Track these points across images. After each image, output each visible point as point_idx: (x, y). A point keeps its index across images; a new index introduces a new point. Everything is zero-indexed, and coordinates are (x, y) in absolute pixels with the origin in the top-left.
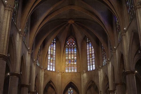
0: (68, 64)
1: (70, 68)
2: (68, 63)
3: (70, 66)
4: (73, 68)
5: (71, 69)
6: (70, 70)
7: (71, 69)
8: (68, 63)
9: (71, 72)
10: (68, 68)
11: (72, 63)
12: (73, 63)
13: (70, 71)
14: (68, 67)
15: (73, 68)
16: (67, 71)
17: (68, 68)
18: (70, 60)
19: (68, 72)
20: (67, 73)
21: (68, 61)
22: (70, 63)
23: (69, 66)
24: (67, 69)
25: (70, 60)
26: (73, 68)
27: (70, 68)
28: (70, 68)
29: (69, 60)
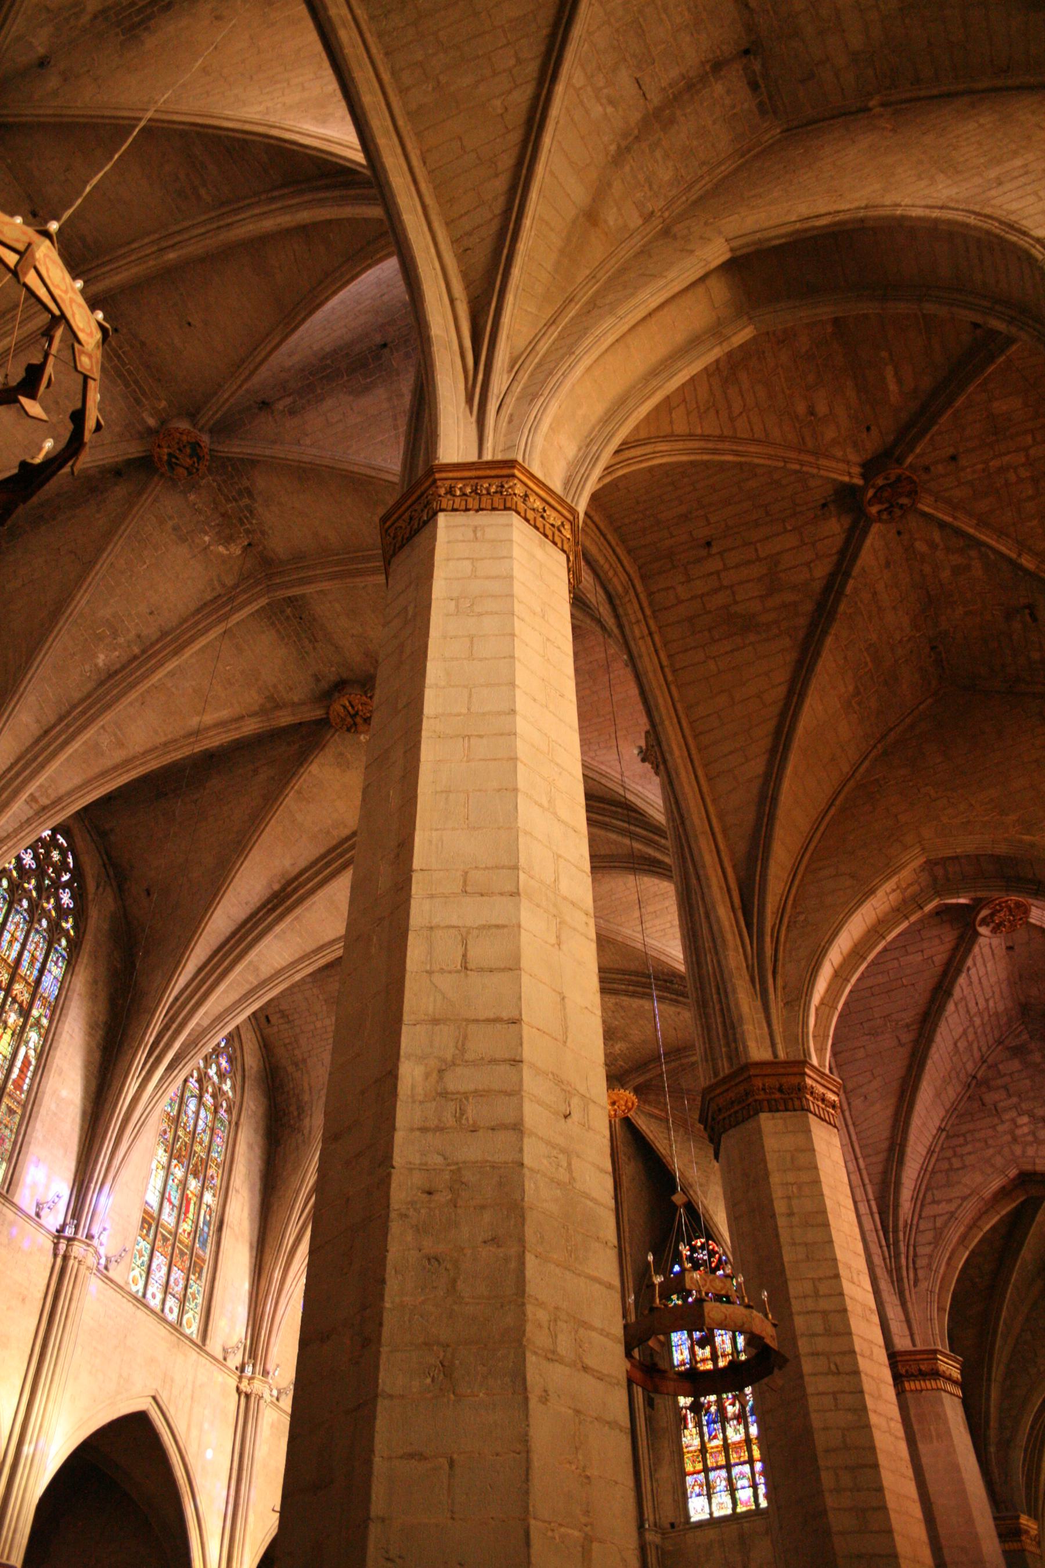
0: (703, 1450)
1: (719, 1478)
2: (701, 1435)
3: (722, 1461)
4: (742, 1476)
5: (732, 1490)
6: (727, 1500)
7: (732, 1490)
8: (697, 1442)
9: (734, 1517)
10: (707, 1477)
11: (730, 1432)
12: (741, 1428)
13: (722, 1506)
14: (706, 1470)
15: (746, 1468)
16: (698, 1509)
17: (707, 1477)
18: (713, 1409)
19: (711, 1514)
20: (701, 1524)
21: (699, 1425)
22: (715, 1437)
23: (710, 1462)
24: (699, 1495)
25: (713, 1409)
26: (746, 1468)
27: (723, 1473)
28: (719, 1478)
29: (708, 1412)
